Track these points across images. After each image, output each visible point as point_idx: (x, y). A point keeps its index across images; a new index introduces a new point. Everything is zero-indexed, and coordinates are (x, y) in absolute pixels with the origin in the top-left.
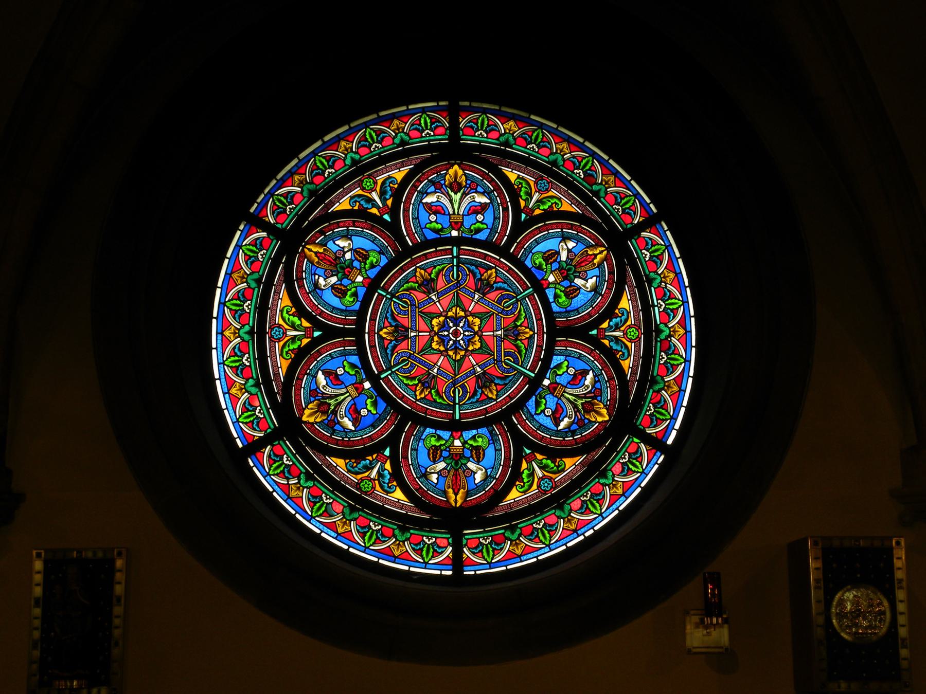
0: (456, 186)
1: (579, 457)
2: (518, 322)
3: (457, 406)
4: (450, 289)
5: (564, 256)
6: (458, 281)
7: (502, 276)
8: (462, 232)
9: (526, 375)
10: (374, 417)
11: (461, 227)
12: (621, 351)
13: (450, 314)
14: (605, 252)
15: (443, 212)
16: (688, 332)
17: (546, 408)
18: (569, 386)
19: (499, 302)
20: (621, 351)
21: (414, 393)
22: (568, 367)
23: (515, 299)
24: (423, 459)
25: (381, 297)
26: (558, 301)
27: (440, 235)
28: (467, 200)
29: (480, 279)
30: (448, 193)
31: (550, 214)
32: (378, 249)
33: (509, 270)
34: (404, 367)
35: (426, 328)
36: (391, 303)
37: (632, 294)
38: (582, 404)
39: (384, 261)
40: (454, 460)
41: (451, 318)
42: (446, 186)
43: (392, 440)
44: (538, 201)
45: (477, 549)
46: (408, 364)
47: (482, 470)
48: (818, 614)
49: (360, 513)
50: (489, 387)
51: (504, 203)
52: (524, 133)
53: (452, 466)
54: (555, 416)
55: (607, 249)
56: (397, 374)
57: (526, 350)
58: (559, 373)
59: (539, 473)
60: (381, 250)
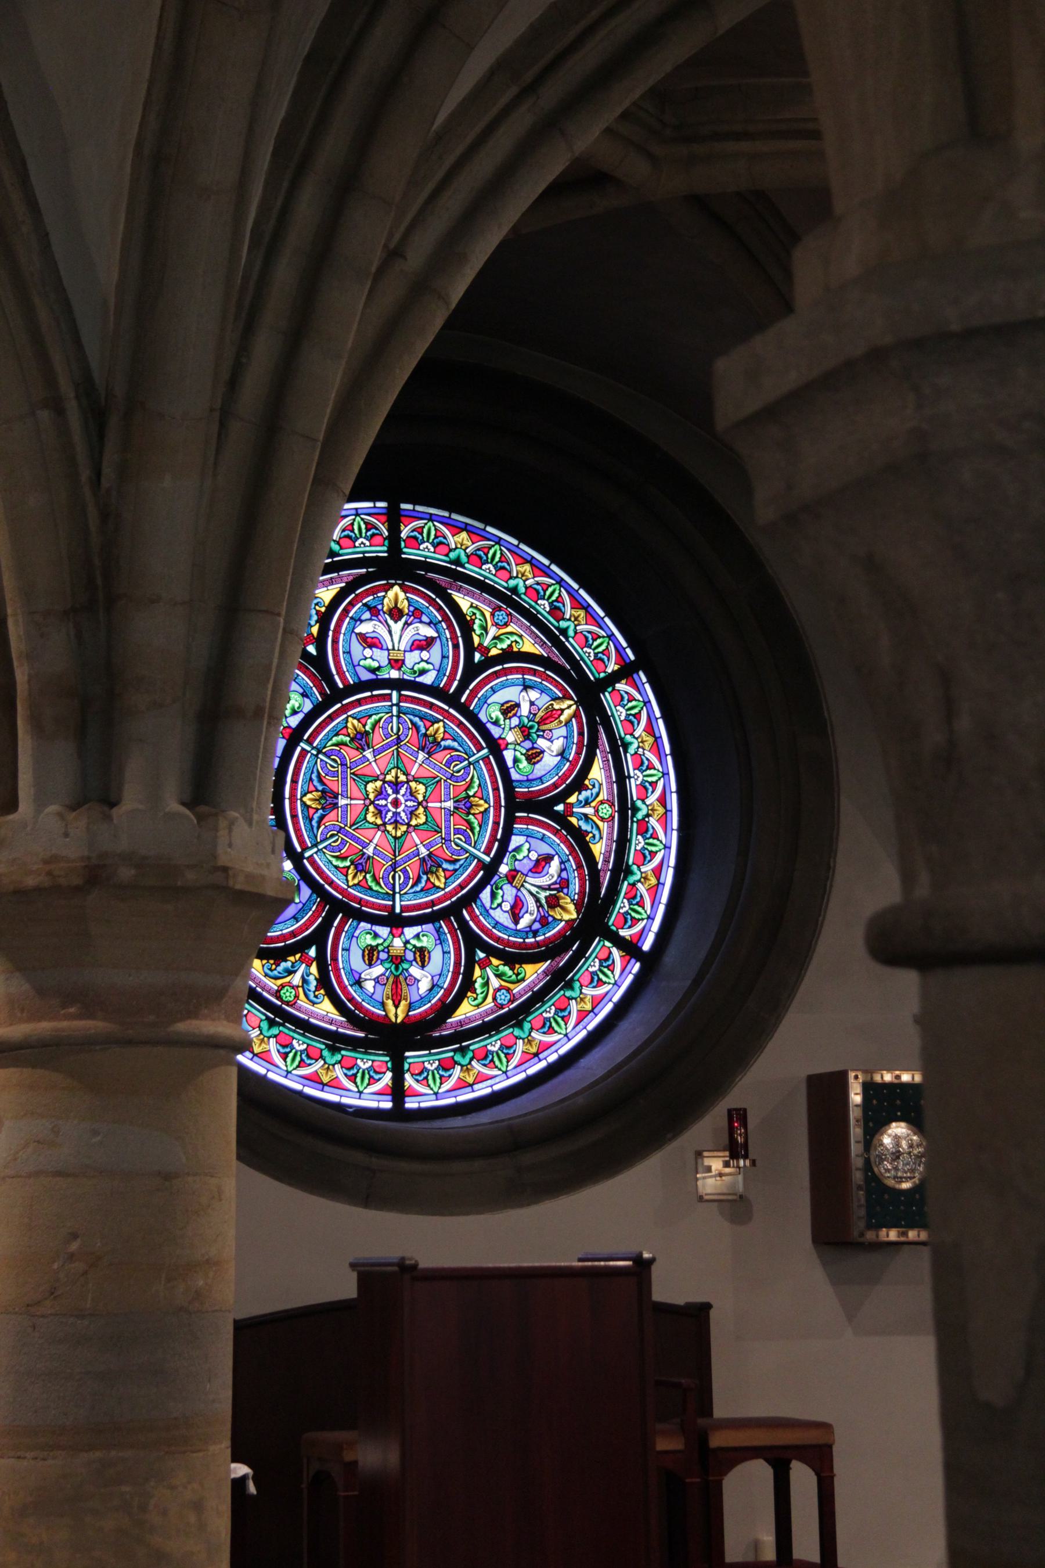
0: (396, 613)
1: (542, 964)
2: (470, 791)
3: (397, 896)
4: (388, 746)
5: (525, 709)
6: (399, 736)
7: (450, 731)
8: (404, 673)
9: (480, 861)
10: (297, 907)
11: (402, 667)
12: (591, 832)
13: (389, 778)
14: (574, 707)
15: (380, 646)
16: (668, 811)
17: (503, 901)
18: (530, 874)
19: (448, 764)
20: (591, 832)
21: (345, 878)
22: (529, 851)
23: (466, 762)
24: (357, 962)
25: (304, 752)
26: (518, 766)
27: (377, 675)
28: (410, 631)
29: (425, 735)
30: (386, 621)
31: (508, 655)
32: (301, 691)
33: (460, 725)
34: (333, 844)
35: (360, 795)
36: (316, 763)
37: (605, 761)
38: (546, 897)
39: (308, 706)
40: (394, 963)
41: (390, 783)
42: (384, 613)
43: (319, 938)
44: (495, 638)
45: (422, 1074)
46: (337, 840)
47: (427, 977)
48: (857, 1156)
49: (281, 1028)
50: (435, 873)
51: (454, 637)
52: (479, 550)
53: (391, 971)
54: (514, 912)
55: (576, 703)
56: (324, 853)
57: (480, 826)
58: (519, 857)
59: (495, 983)
60: (305, 691)
